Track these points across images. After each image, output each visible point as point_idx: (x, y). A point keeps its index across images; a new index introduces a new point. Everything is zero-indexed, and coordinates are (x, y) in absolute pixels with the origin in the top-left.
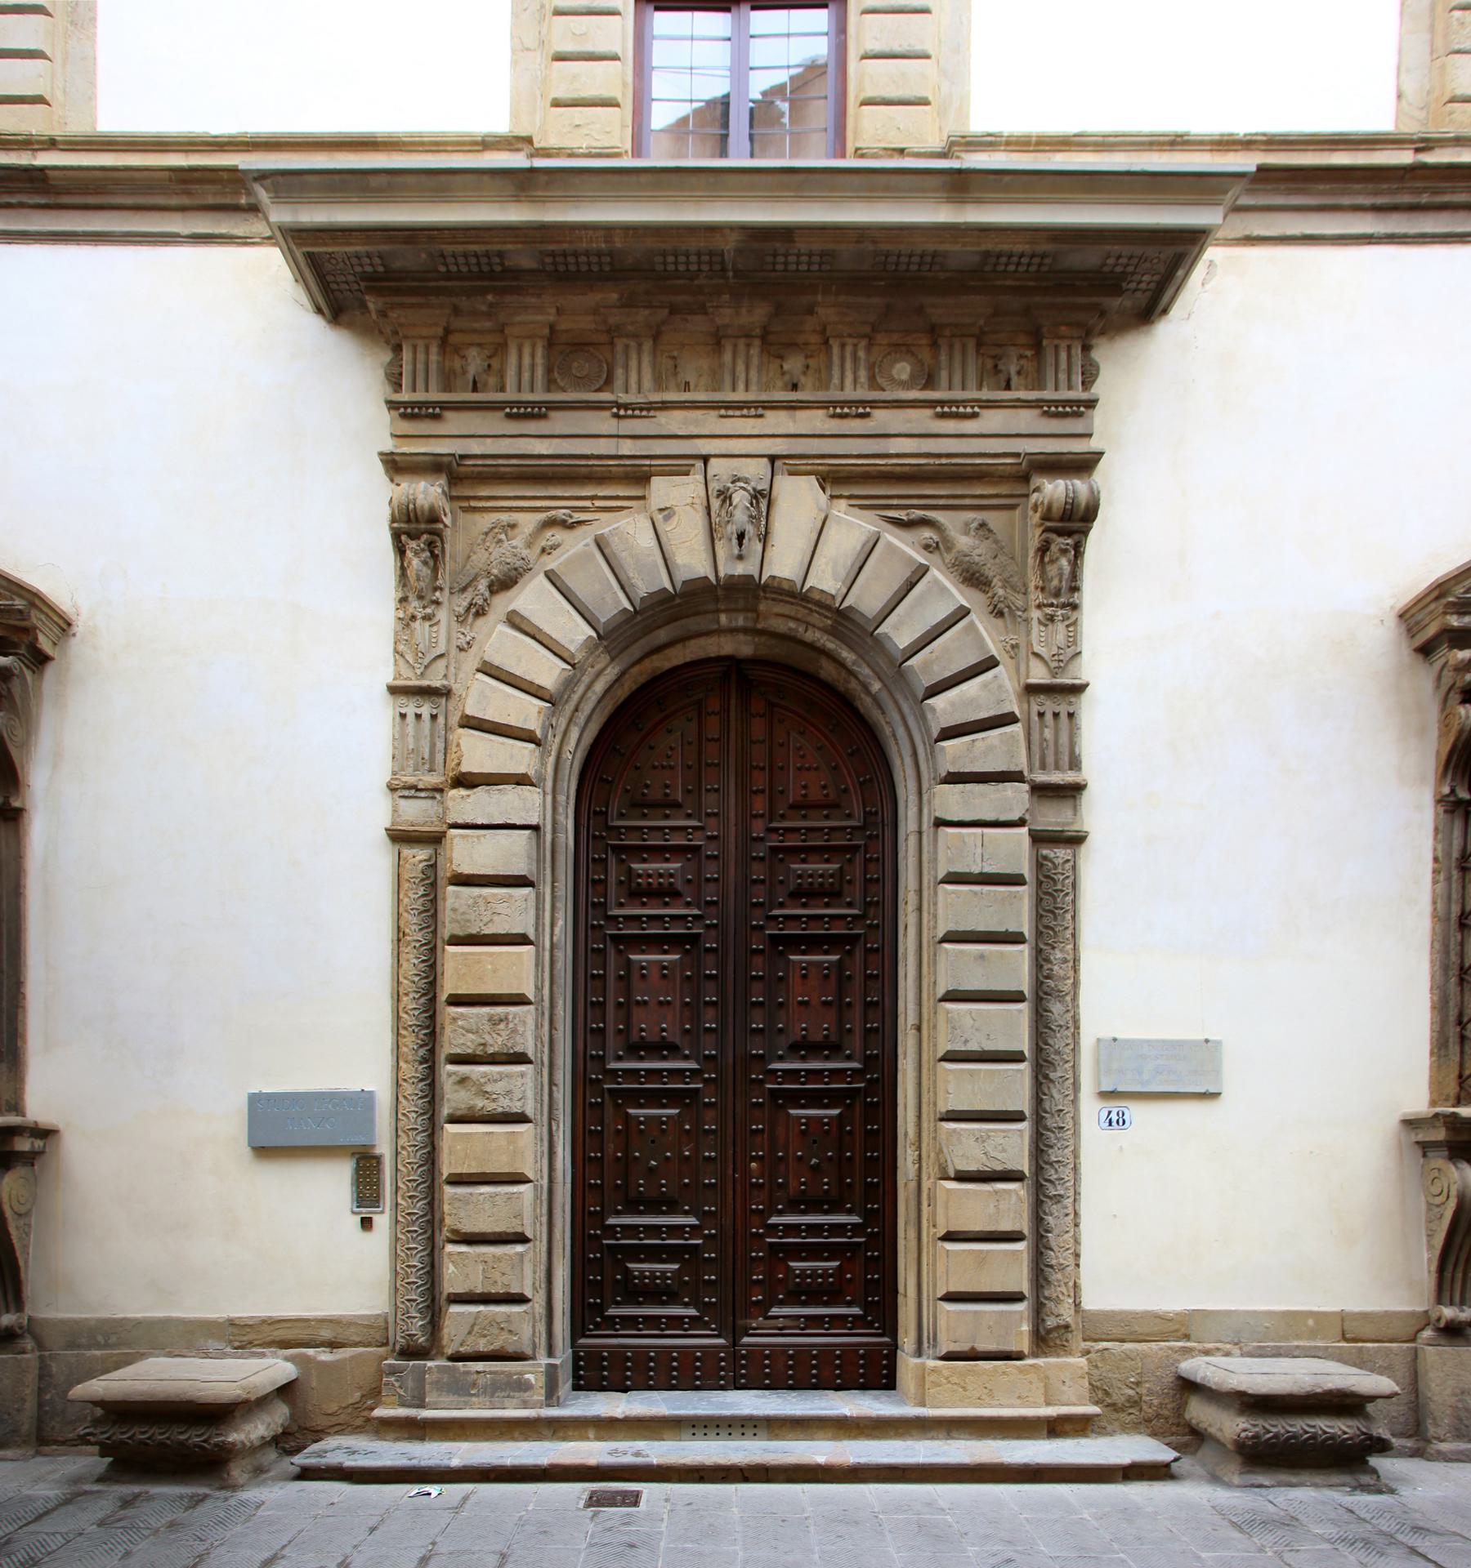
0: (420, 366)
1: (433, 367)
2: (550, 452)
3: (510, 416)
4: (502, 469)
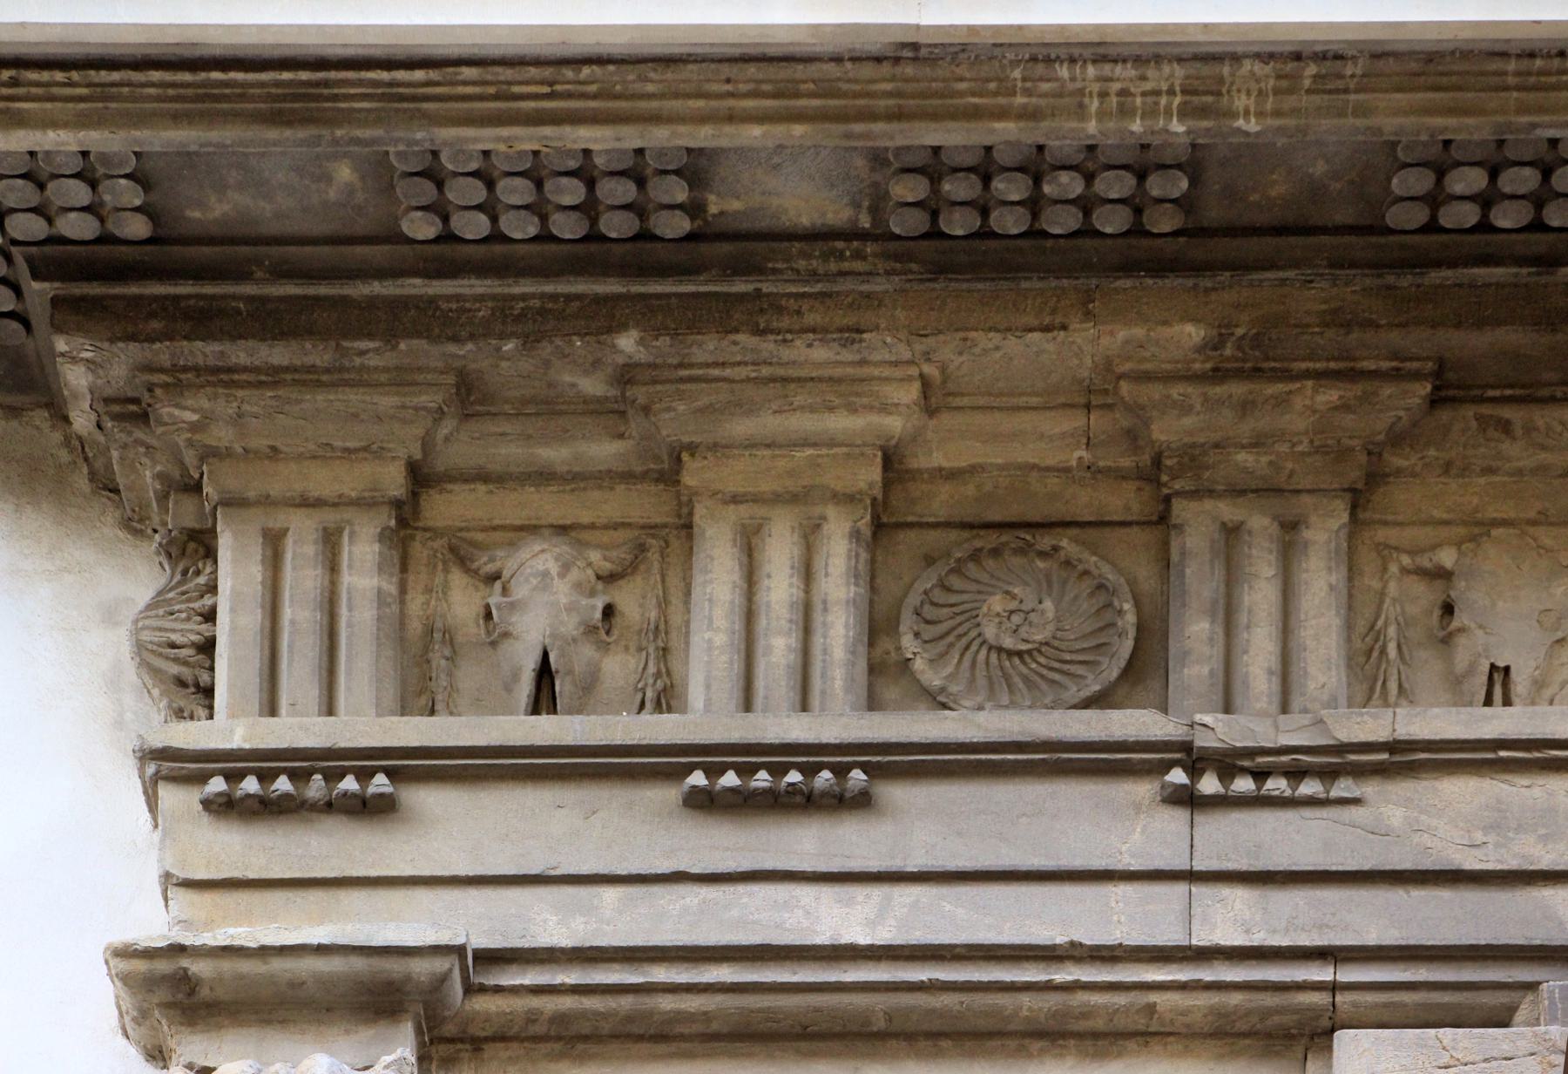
0: (299, 615)
1: (360, 619)
2: (885, 935)
3: (704, 803)
4: (667, 1003)
